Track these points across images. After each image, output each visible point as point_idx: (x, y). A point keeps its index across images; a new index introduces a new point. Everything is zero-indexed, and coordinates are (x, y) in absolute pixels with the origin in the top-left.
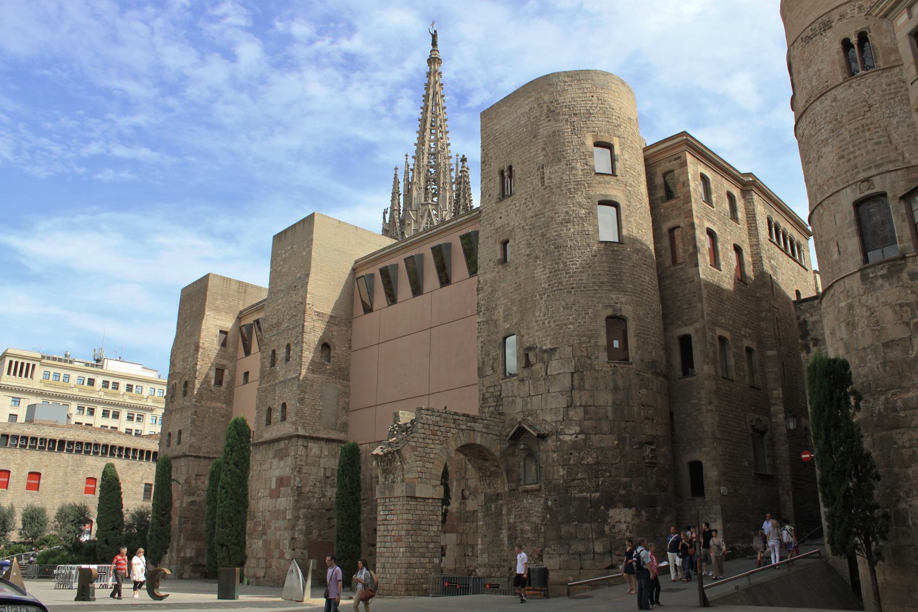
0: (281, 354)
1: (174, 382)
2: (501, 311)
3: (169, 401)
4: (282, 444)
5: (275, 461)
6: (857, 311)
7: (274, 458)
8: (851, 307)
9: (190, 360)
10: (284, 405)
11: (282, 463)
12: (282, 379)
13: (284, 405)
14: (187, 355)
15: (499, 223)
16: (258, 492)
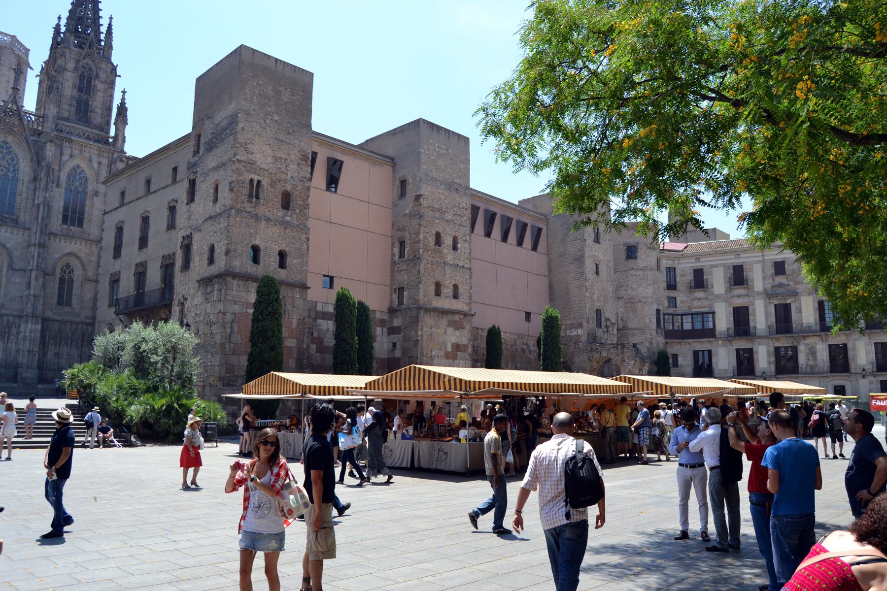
0: (448, 241)
1: (256, 178)
2: (596, 295)
3: (244, 198)
4: (457, 318)
5: (450, 330)
6: (654, 340)
7: (448, 325)
8: (652, 339)
9: (292, 166)
10: (456, 287)
11: (458, 333)
12: (451, 263)
13: (456, 287)
14: (284, 156)
15: (595, 253)
16: (432, 352)
